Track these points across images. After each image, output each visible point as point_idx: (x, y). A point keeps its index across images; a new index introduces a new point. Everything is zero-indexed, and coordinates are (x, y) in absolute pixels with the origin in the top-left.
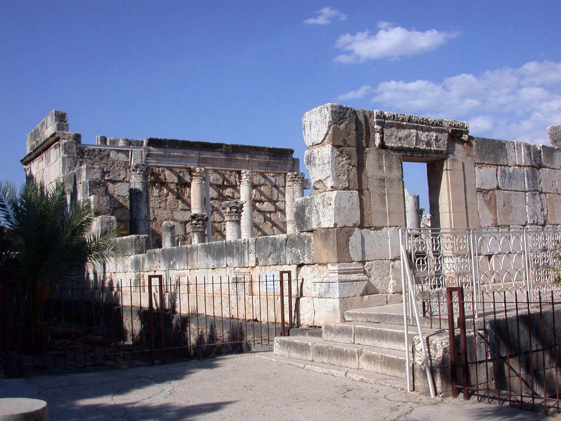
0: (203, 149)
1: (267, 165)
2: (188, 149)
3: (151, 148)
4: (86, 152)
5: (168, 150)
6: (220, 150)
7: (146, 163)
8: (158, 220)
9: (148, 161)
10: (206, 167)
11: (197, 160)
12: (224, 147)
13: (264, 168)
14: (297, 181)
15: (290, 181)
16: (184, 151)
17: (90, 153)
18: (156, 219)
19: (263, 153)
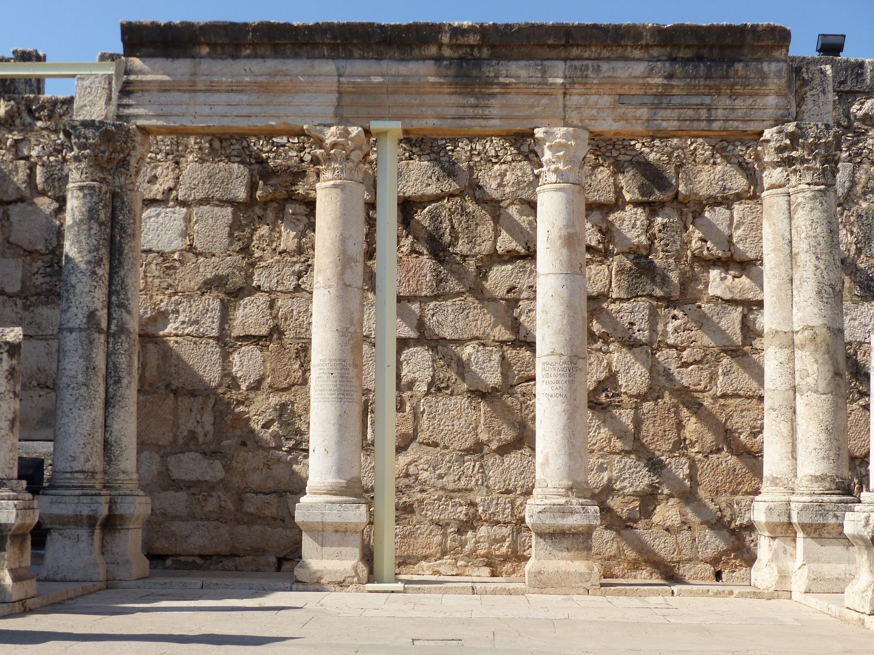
0: (357, 53)
1: (660, 99)
2: (296, 56)
3: (136, 62)
4: (42, 108)
5: (206, 65)
6: (433, 50)
7: (119, 117)
8: (289, 334)
9: (127, 111)
10: (375, 126)
11: (334, 97)
12: (445, 39)
13: (644, 112)
14: (803, 161)
15: (777, 164)
16: (272, 64)
17: (59, 111)
18: (282, 333)
19: (637, 53)
